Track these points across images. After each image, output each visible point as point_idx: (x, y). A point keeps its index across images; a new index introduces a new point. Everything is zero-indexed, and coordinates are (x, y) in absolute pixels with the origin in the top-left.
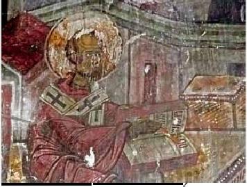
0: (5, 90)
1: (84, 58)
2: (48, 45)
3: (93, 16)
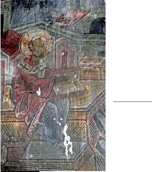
0: (2, 63)
1: (36, 49)
2: (21, 43)
3: (40, 31)
